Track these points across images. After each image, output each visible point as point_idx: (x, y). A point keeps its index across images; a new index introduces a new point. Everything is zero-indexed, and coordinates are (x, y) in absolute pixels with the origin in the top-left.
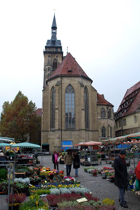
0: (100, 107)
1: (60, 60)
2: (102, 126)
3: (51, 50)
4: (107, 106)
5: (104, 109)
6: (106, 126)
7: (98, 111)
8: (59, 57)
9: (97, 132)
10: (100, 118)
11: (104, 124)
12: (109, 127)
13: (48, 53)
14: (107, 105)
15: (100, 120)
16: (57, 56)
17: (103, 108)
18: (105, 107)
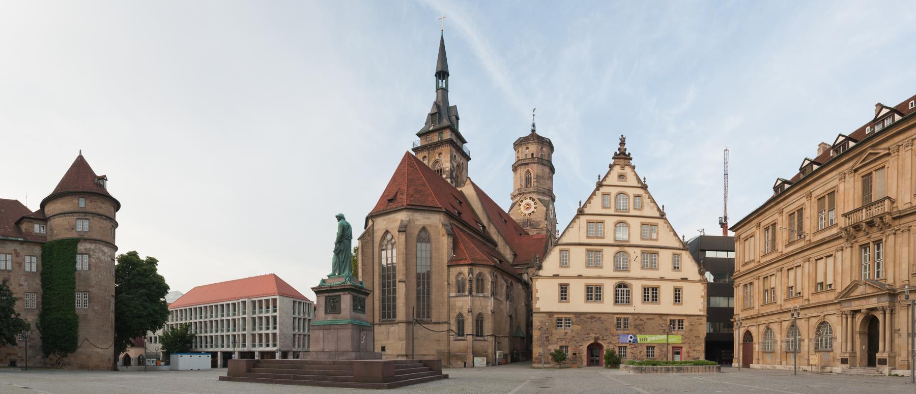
0: (455, 271)
1: (447, 162)
2: (457, 311)
3: (435, 138)
4: (470, 267)
5: (464, 275)
6: (465, 312)
7: (450, 281)
8: (444, 154)
9: (446, 325)
10: (452, 294)
11: (461, 308)
12: (470, 314)
13: (422, 150)
14: (468, 265)
15: (453, 299)
16: (440, 154)
17: (460, 273)
18: (465, 270)
